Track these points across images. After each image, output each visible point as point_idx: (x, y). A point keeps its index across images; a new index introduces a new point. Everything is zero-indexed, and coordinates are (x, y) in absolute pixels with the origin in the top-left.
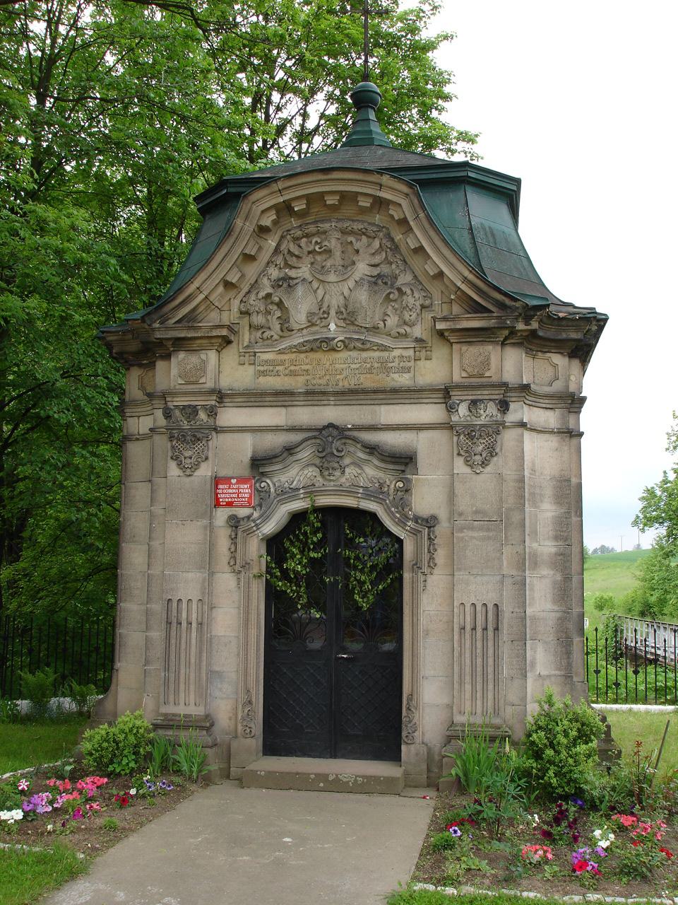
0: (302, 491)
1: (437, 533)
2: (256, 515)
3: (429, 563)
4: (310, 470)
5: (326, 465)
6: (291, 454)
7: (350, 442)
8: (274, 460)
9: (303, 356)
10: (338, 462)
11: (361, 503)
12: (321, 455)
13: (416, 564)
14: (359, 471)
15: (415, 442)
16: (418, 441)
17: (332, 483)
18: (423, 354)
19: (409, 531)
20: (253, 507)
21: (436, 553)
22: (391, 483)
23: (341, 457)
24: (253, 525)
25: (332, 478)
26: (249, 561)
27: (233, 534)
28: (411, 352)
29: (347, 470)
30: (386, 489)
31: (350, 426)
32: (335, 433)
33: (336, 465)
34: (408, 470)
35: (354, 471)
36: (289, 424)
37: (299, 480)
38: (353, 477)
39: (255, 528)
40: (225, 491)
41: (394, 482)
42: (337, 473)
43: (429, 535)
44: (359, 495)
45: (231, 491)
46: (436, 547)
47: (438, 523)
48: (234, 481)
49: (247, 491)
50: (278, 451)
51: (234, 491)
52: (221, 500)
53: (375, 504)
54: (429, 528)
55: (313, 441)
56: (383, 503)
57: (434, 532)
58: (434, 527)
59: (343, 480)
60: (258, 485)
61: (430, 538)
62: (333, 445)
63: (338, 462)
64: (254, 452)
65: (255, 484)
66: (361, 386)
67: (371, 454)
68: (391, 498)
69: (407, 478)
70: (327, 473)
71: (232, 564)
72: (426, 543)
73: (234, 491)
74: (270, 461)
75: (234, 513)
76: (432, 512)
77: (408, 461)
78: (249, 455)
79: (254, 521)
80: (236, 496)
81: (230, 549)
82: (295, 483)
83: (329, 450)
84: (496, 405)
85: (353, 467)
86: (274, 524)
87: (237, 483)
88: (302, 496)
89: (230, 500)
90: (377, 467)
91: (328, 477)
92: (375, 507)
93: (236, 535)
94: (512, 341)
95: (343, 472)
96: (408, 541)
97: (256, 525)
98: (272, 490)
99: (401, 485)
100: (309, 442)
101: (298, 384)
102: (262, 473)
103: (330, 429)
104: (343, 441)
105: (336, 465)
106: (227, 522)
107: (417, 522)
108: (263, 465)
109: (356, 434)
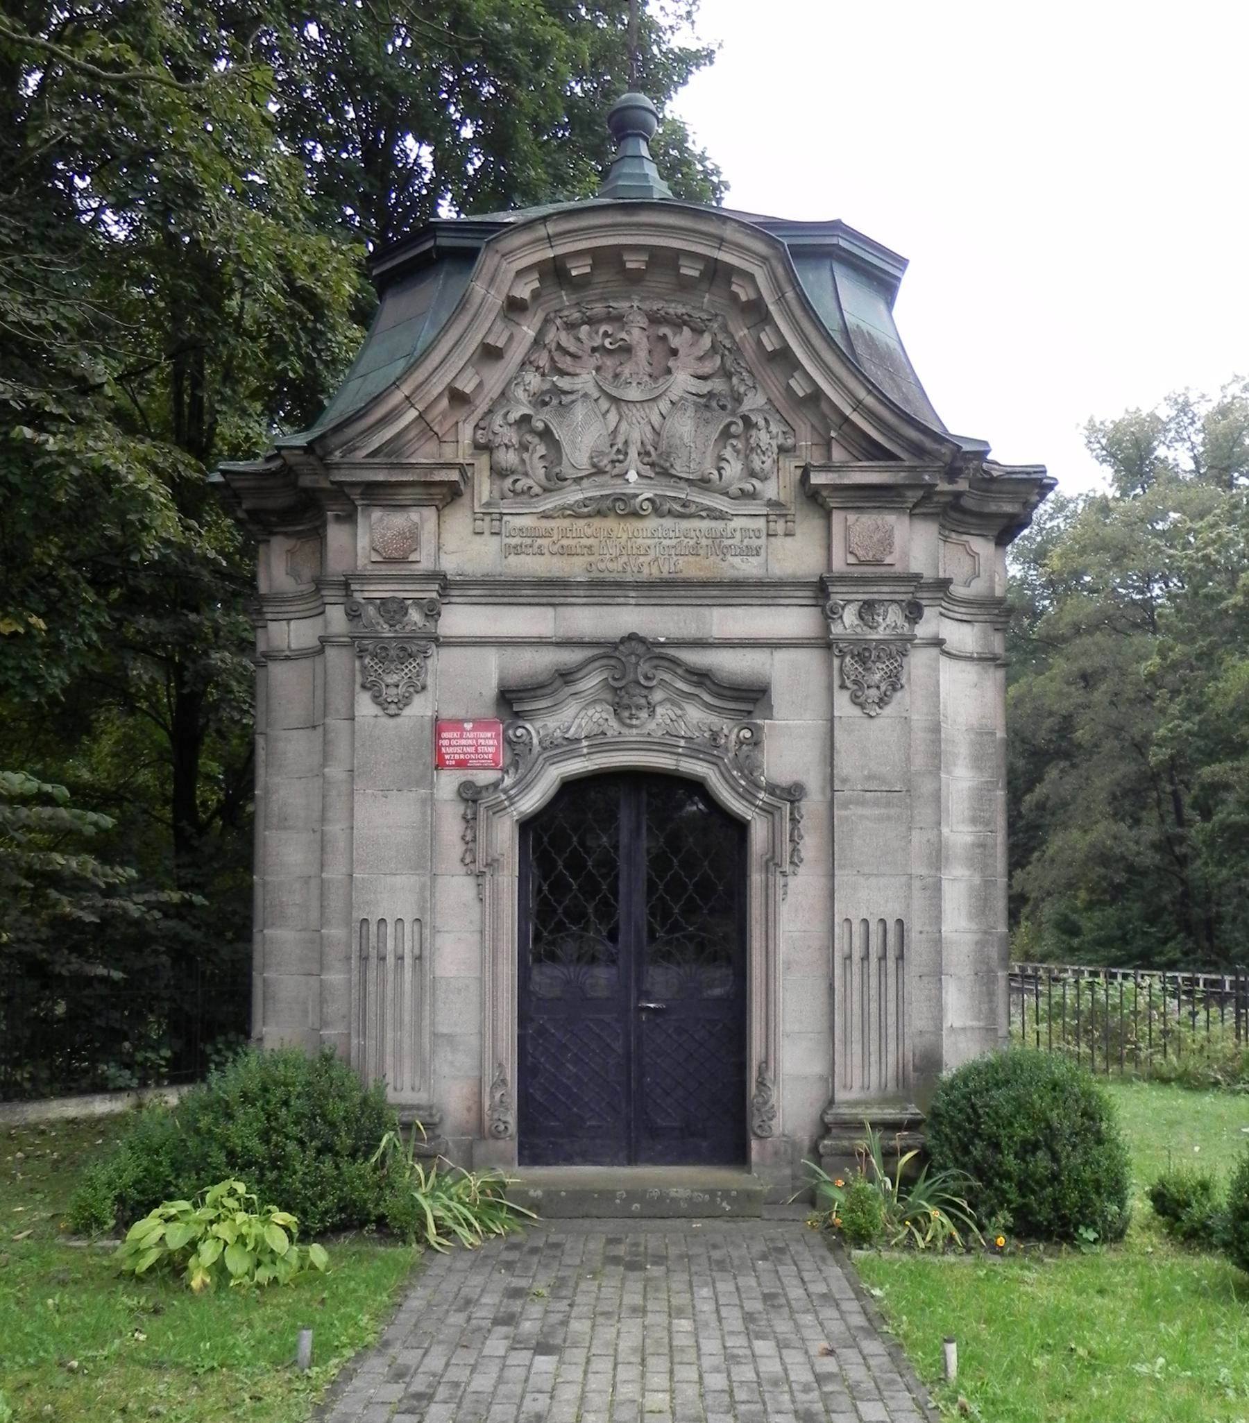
0: (585, 743)
1: (803, 811)
2: (508, 781)
3: (792, 857)
4: (599, 709)
5: (626, 701)
7: (666, 664)
8: (539, 692)
10: (646, 697)
11: (682, 764)
12: (617, 684)
13: (773, 858)
14: (679, 712)
15: (767, 666)
16: (772, 665)
17: (634, 731)
19: (761, 808)
20: (501, 769)
21: (801, 842)
22: (730, 731)
23: (651, 688)
24: (503, 797)
25: (634, 722)
26: (497, 856)
27: (469, 812)
29: (659, 710)
30: (723, 741)
31: (662, 640)
32: (641, 649)
33: (643, 701)
34: (757, 713)
35: (670, 712)
36: (560, 634)
37: (580, 726)
38: (669, 721)
39: (506, 803)
41: (736, 730)
42: (644, 714)
43: (791, 813)
44: (680, 750)
45: (464, 742)
46: (802, 832)
47: (806, 795)
48: (468, 726)
49: (491, 742)
50: (541, 678)
51: (470, 742)
52: (447, 757)
53: (705, 764)
54: (792, 802)
55: (604, 662)
56: (720, 763)
57: (799, 808)
58: (799, 800)
59: (652, 726)
60: (511, 732)
61: (792, 819)
62: (639, 669)
63: (646, 697)
64: (501, 679)
65: (505, 731)
67: (699, 684)
68: (731, 755)
69: (755, 724)
70: (626, 714)
71: (467, 861)
72: (788, 826)
74: (532, 693)
75: (470, 778)
76: (796, 778)
77: (759, 696)
78: (494, 682)
79: (505, 791)
81: (463, 838)
82: (573, 730)
83: (631, 677)
85: (669, 706)
86: (538, 796)
87: (474, 729)
88: (585, 751)
89: (462, 757)
90: (708, 706)
91: (628, 721)
92: (705, 770)
93: (475, 814)
95: (652, 713)
96: (759, 823)
97: (510, 798)
98: (535, 741)
99: (748, 734)
100: (597, 664)
102: (517, 713)
103: (633, 643)
104: (655, 662)
105: (643, 701)
106: (459, 793)
107: (772, 793)
108: (521, 700)
109: (672, 652)
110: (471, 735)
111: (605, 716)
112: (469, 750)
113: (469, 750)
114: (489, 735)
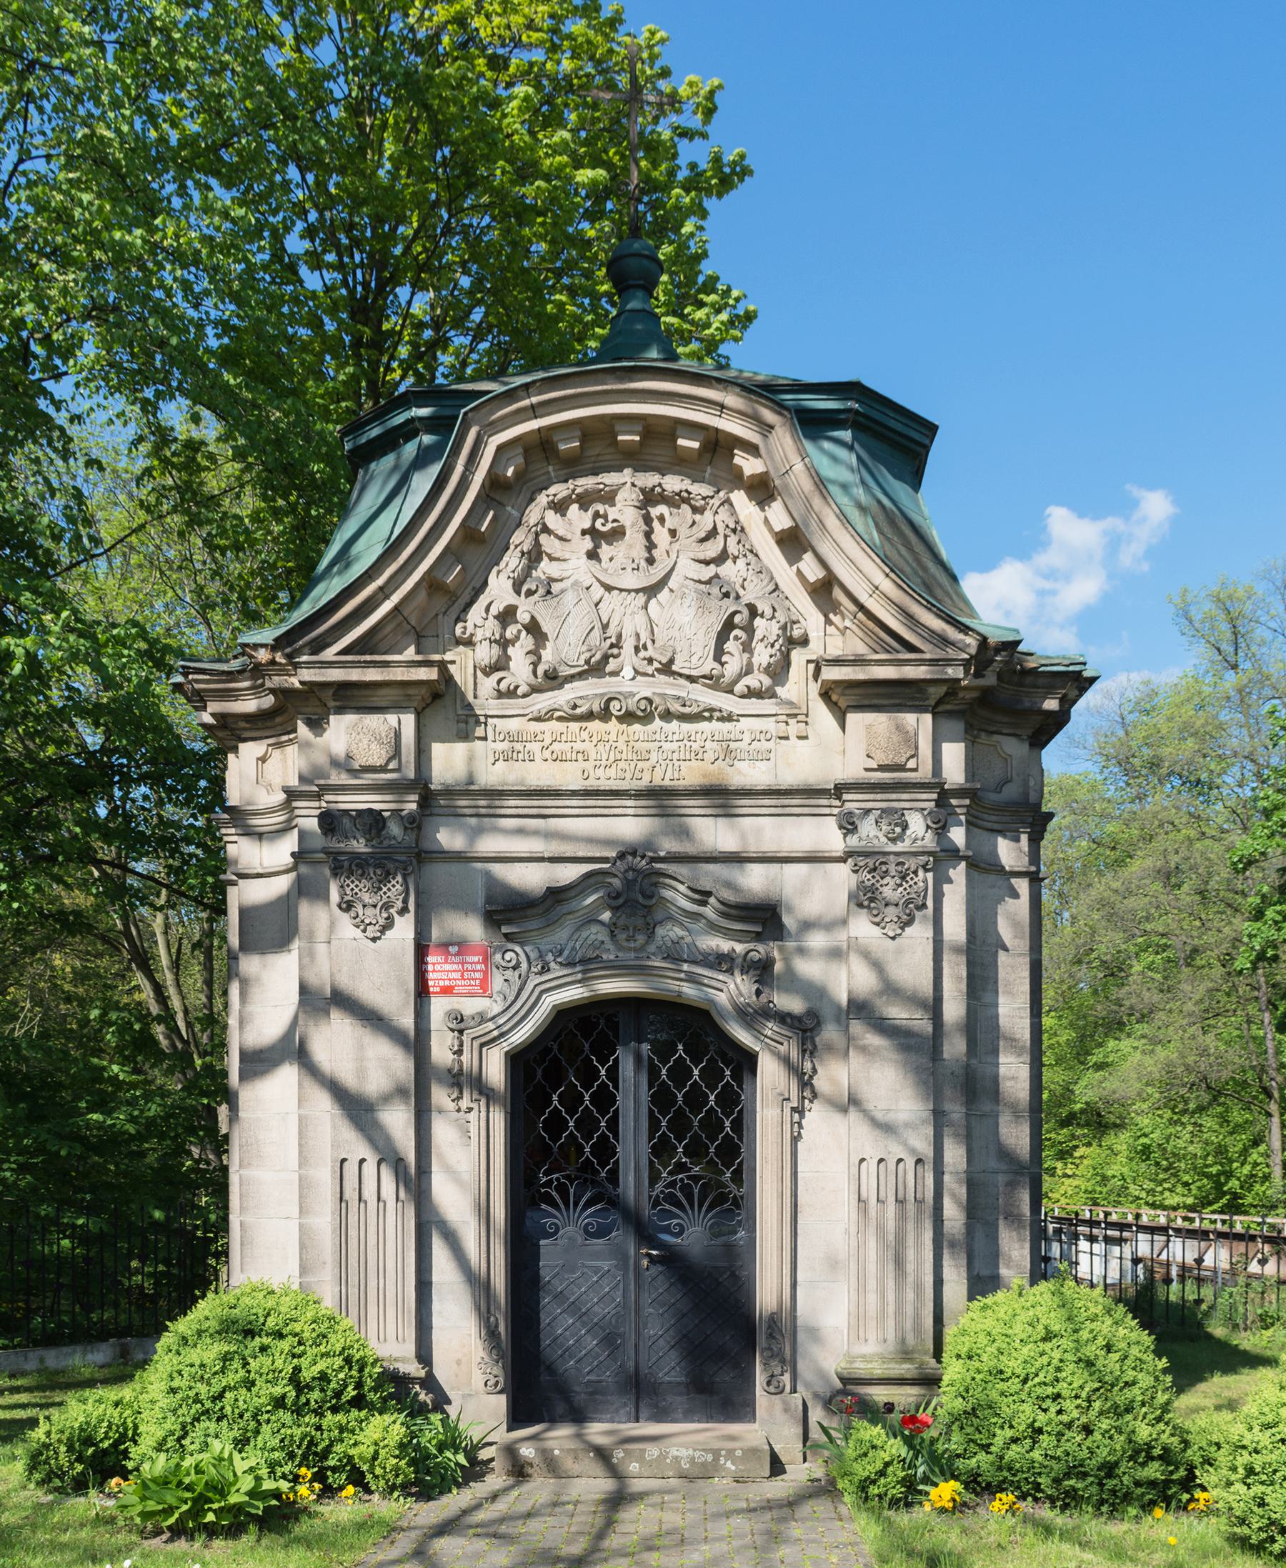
6: (559, 902)
8: (529, 912)
9: (574, 726)
18: (794, 728)
28: (769, 724)
37: (573, 948)
40: (438, 967)
54: (804, 1031)
66: (681, 782)
73: (455, 967)
75: (456, 1006)
78: (480, 901)
80: (458, 975)
82: (566, 953)
84: (925, 817)
94: (949, 707)
101: (568, 777)
102: (506, 935)
110: (457, 959)
111: (600, 937)
112: (455, 975)
113: (455, 975)
114: (476, 959)
